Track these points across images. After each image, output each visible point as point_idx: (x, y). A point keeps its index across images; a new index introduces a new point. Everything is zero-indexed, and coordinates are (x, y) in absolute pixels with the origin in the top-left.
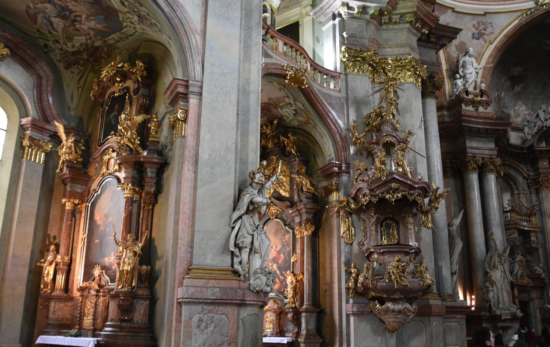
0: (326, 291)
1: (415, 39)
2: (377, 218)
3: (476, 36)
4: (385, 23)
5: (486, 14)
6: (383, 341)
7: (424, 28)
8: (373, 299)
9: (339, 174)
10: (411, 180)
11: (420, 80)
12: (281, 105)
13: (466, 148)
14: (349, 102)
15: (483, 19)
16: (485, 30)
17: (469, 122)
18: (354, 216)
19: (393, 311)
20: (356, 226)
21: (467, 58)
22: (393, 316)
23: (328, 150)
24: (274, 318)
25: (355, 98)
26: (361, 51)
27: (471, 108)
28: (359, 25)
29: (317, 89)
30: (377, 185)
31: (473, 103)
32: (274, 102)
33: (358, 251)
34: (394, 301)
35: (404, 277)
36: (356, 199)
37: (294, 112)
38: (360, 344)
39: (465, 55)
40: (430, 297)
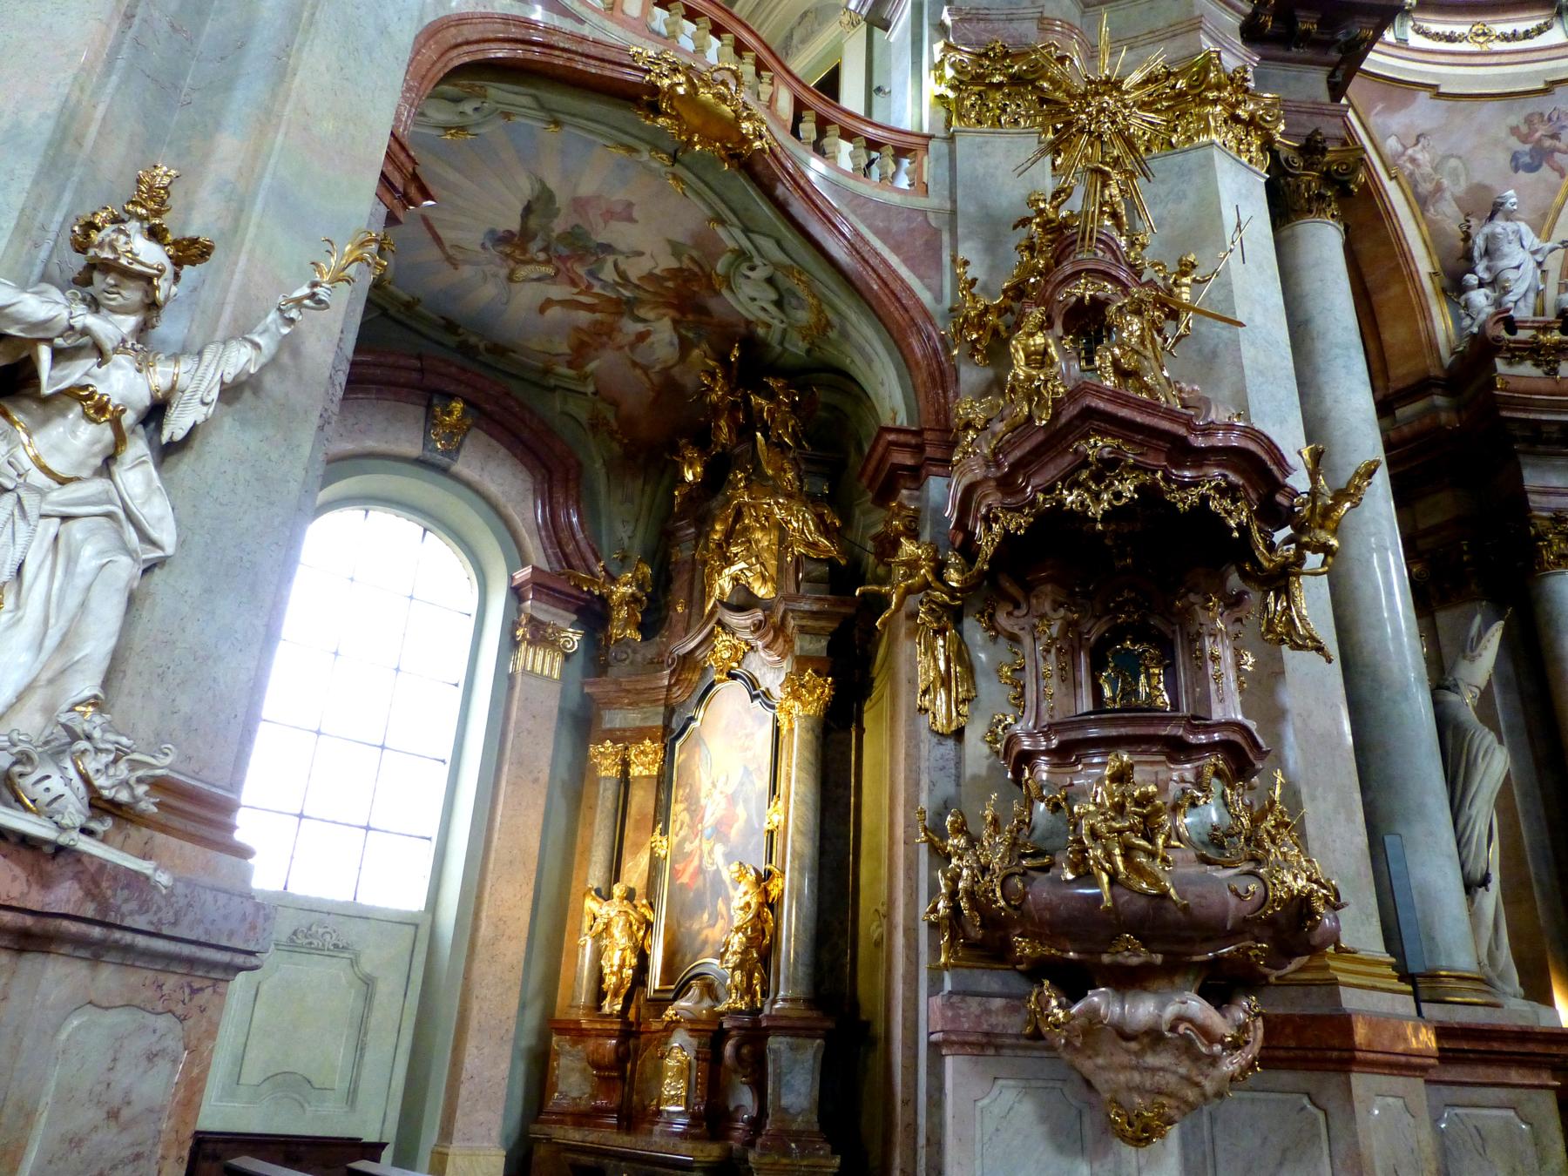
0: (878, 944)
2: (1069, 625)
3: (1527, 159)
5: (1550, 87)
8: (1037, 971)
9: (916, 476)
10: (1170, 414)
12: (720, 267)
13: (1525, 493)
15: (1546, 105)
16: (1555, 136)
17: (1526, 405)
19: (1123, 1034)
21: (1499, 226)
22: (1126, 1059)
23: (890, 397)
24: (691, 1057)
27: (1527, 369)
30: (1017, 454)
31: (1533, 351)
32: (692, 259)
33: (986, 763)
34: (1128, 980)
35: (1152, 855)
36: (968, 550)
37: (774, 296)
39: (1491, 218)
40: (1341, 978)
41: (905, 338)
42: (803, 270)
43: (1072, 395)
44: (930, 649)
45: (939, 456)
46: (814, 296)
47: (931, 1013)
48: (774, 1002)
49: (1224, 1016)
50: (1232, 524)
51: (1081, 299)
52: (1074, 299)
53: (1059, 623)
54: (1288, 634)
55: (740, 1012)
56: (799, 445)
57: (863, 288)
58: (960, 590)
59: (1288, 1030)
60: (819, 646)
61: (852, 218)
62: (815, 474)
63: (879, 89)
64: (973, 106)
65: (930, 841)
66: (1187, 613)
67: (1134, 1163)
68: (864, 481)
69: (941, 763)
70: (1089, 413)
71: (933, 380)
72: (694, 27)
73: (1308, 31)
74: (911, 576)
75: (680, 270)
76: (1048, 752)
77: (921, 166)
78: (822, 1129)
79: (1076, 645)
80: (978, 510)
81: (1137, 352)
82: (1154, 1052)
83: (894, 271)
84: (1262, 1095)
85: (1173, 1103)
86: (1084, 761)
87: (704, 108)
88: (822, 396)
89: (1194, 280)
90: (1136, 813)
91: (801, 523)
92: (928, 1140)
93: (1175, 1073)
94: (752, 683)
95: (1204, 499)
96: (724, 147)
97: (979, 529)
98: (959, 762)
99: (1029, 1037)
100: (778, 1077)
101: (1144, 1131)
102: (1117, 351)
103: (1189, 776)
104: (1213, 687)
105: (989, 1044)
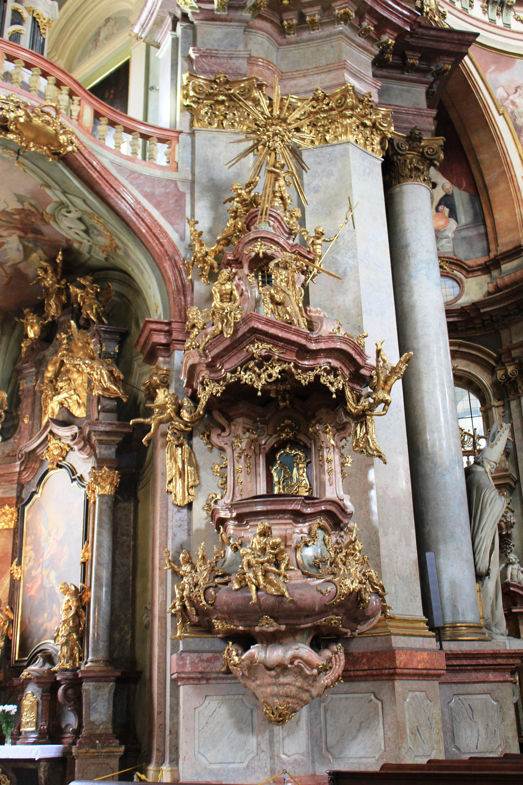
1: (368, 59)
4: (290, 27)
6: (264, 746)
7: (384, 33)
11: (377, 139)
12: (49, 209)
14: (197, 188)
18: (198, 442)
20: (200, 463)
22: (269, 680)
25: (211, 180)
26: (227, 82)
28: (227, 34)
29: (112, 163)
30: (216, 351)
32: (30, 204)
33: (205, 522)
34: (272, 639)
36: (194, 398)
37: (83, 227)
38: (200, 757)
40: (393, 630)
41: (162, 263)
42: (100, 217)
43: (245, 320)
44: (173, 457)
45: (180, 338)
46: (108, 231)
47: (172, 661)
48: (86, 663)
49: (320, 655)
50: (333, 389)
51: (257, 254)
52: (253, 254)
53: (246, 441)
54: (366, 448)
55: (66, 670)
56: (101, 322)
57: (136, 230)
58: (191, 422)
59: (365, 660)
60: (110, 452)
61: (130, 187)
62: (110, 340)
63: (152, 88)
64: (206, 113)
65: (172, 568)
66: (315, 437)
67: (281, 736)
68: (139, 349)
69: (179, 523)
70: (254, 331)
71: (178, 290)
72: (30, 72)
73: (413, 64)
74: (162, 413)
75: (23, 210)
76: (231, 519)
77: (174, 150)
78: (114, 732)
79: (257, 451)
80: (198, 378)
81: (284, 292)
82: (284, 676)
83: (155, 221)
84: (352, 695)
85: (295, 701)
86: (251, 523)
87: (37, 130)
88: (114, 286)
89: (324, 241)
90: (271, 553)
91: (101, 375)
92: (170, 731)
93: (294, 685)
94: (72, 471)
95: (317, 377)
96: (49, 149)
97: (200, 388)
98: (190, 522)
99: (224, 673)
100: (89, 704)
101: (280, 716)
102: (272, 291)
103: (305, 530)
104: (327, 477)
105: (202, 678)
